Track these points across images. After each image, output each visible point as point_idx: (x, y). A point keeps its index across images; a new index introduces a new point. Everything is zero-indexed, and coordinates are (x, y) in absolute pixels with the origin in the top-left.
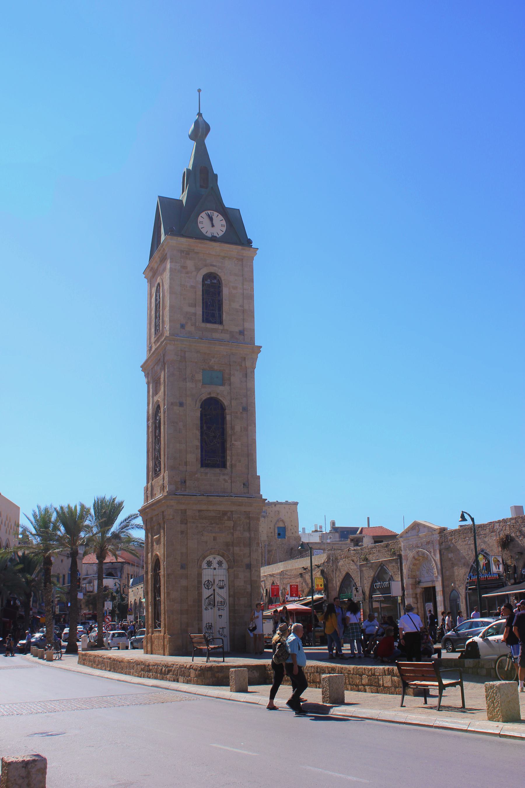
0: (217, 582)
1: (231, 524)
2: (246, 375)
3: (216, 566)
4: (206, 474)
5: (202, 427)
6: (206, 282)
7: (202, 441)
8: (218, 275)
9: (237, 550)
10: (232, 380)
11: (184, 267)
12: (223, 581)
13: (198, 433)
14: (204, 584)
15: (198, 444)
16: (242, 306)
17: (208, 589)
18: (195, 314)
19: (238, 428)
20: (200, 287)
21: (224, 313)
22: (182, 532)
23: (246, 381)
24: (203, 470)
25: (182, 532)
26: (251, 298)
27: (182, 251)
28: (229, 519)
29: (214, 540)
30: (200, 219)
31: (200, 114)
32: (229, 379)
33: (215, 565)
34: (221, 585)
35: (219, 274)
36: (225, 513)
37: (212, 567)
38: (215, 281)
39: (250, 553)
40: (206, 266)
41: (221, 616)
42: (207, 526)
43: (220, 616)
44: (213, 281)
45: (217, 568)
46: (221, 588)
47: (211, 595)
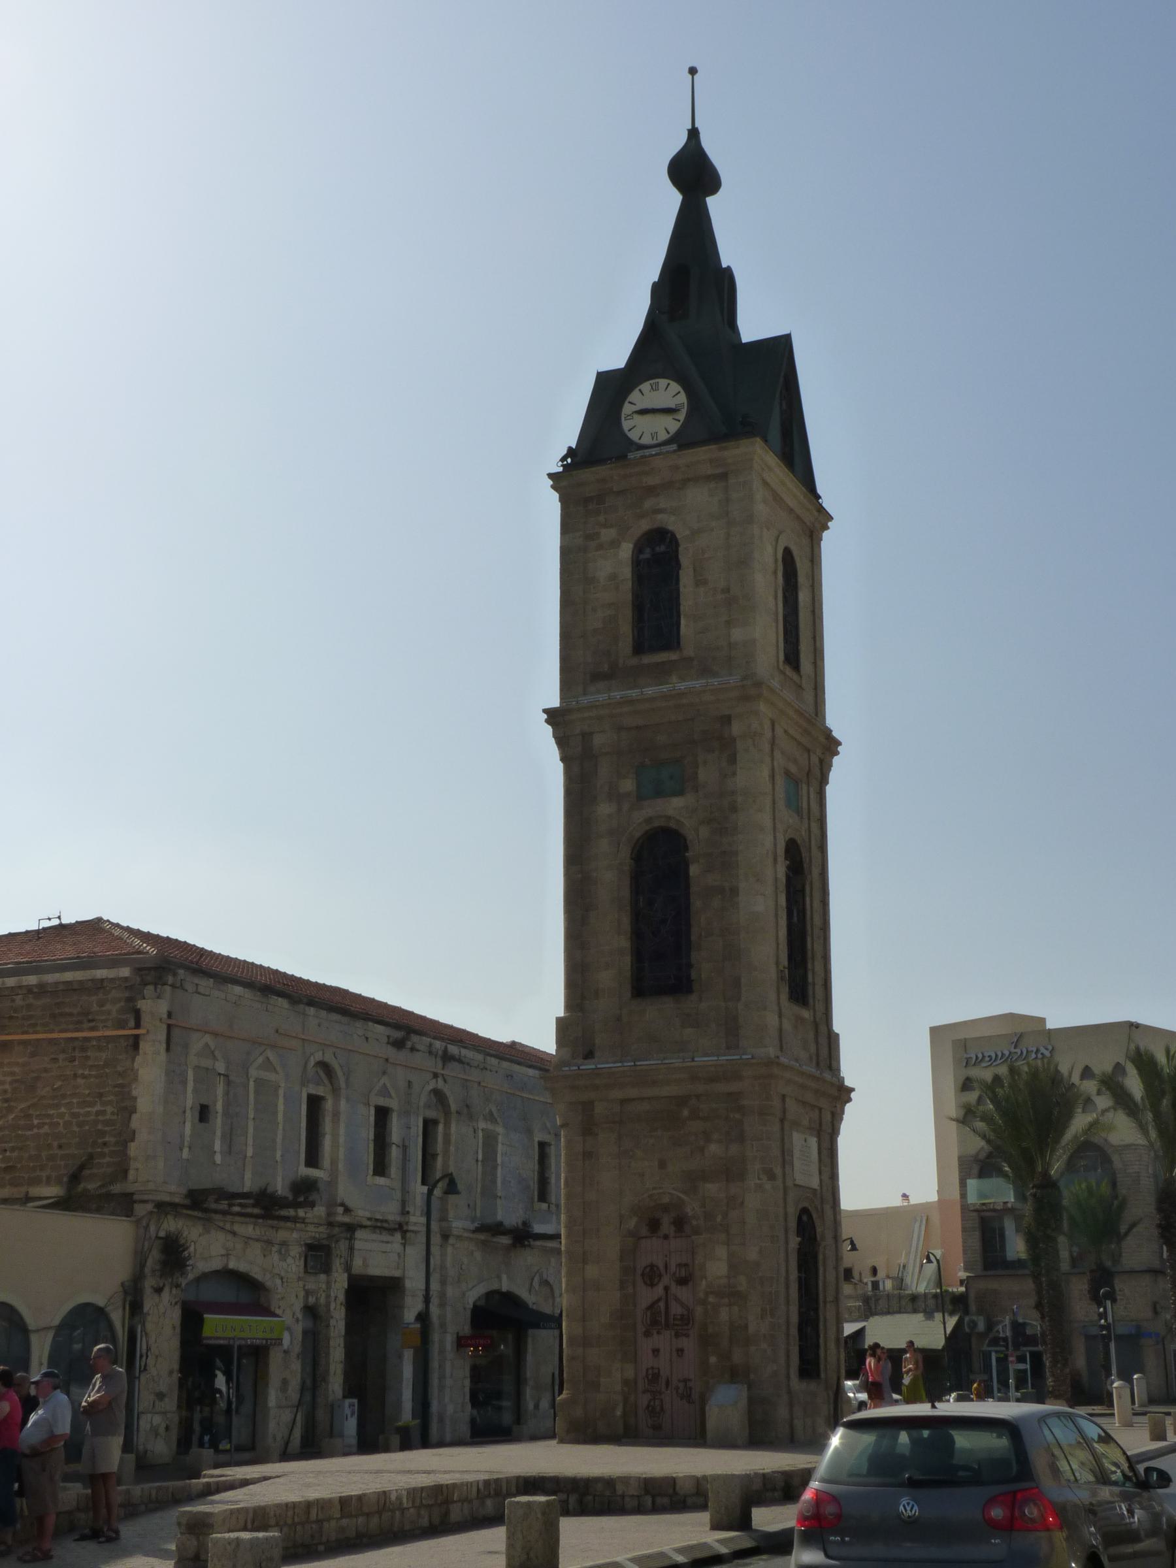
0: (673, 1268)
2: (733, 760)
6: (642, 557)
7: (637, 935)
9: (712, 1189)
12: (686, 1265)
14: (643, 1275)
15: (625, 943)
17: (652, 1285)
20: (627, 572)
22: (588, 1155)
23: (734, 774)
30: (627, 409)
33: (666, 1227)
34: (683, 1274)
35: (670, 528)
36: (682, 1101)
38: (662, 548)
41: (682, 1350)
43: (680, 1352)
44: (658, 549)
46: (683, 1282)
47: (659, 1300)
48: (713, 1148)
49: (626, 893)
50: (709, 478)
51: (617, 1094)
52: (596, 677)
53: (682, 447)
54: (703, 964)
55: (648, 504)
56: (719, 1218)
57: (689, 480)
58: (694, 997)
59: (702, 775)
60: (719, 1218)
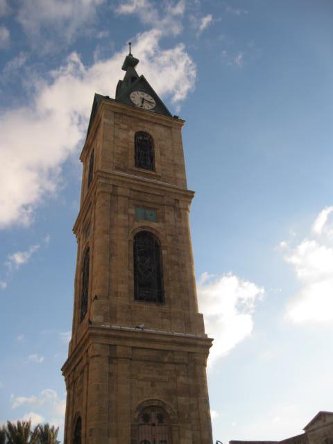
1: (171, 367)
2: (180, 216)
3: (156, 422)
4: (143, 307)
8: (149, 134)
9: (182, 399)
13: (132, 265)
15: (132, 275)
16: (173, 161)
20: (133, 140)
24: (136, 303)
25: (111, 374)
26: (181, 154)
27: (115, 113)
29: (152, 386)
31: (130, 55)
32: (163, 217)
33: (154, 420)
39: (198, 404)
40: (138, 126)
45: (157, 424)
48: (181, 379)
49: (132, 253)
50: (164, 126)
51: (131, 344)
52: (118, 168)
54: (170, 291)
55: (141, 124)
56: (186, 416)
57: (156, 123)
58: (167, 306)
59: (167, 217)
60: (186, 416)
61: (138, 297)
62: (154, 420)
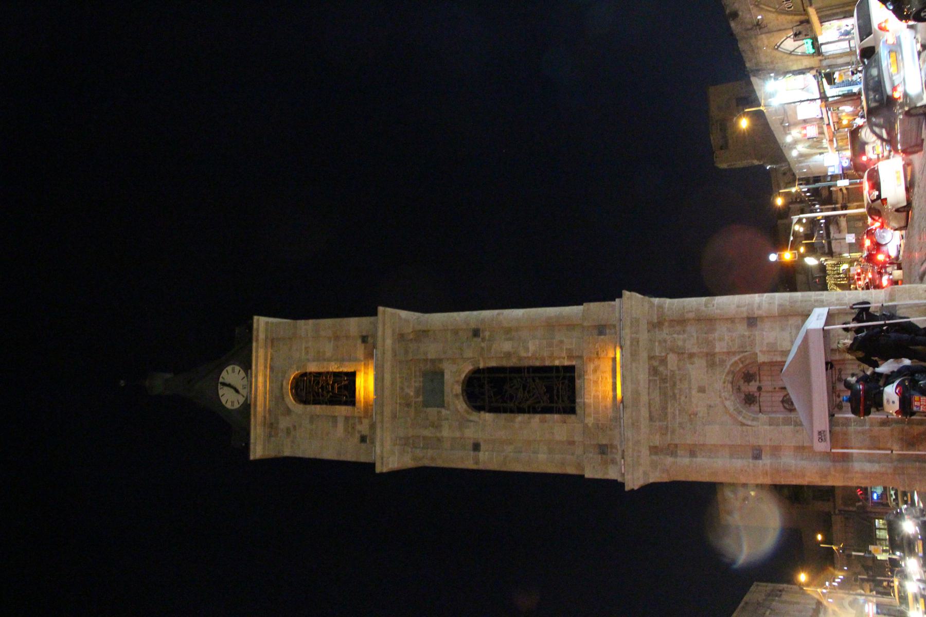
1: (672, 358)
5: (512, 411)
7: (533, 410)
10: (434, 357)
11: (288, 431)
13: (520, 418)
15: (537, 417)
18: (347, 418)
19: (507, 346)
21: (341, 370)
27: (270, 436)
28: (663, 361)
32: (433, 361)
36: (654, 371)
37: (757, 394)
42: (680, 404)
45: (757, 383)
48: (691, 346)
49: (503, 416)
53: (250, 367)
59: (431, 356)
61: (572, 411)
62: (752, 387)
